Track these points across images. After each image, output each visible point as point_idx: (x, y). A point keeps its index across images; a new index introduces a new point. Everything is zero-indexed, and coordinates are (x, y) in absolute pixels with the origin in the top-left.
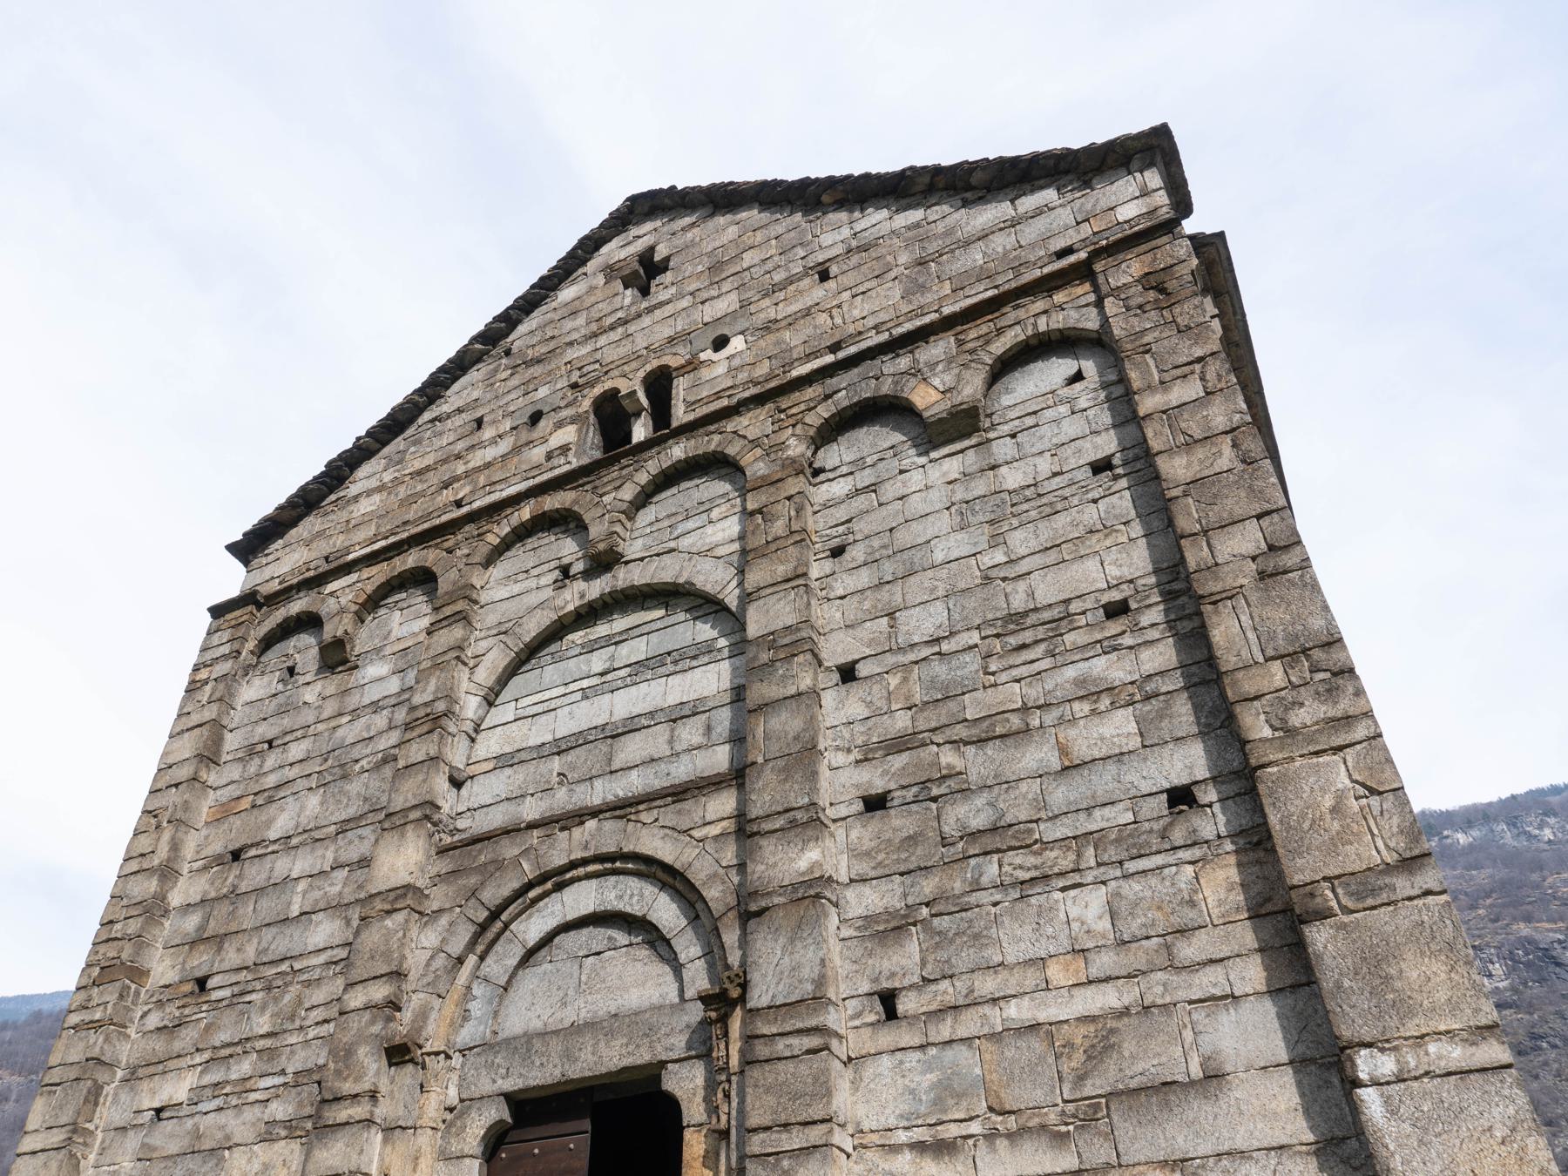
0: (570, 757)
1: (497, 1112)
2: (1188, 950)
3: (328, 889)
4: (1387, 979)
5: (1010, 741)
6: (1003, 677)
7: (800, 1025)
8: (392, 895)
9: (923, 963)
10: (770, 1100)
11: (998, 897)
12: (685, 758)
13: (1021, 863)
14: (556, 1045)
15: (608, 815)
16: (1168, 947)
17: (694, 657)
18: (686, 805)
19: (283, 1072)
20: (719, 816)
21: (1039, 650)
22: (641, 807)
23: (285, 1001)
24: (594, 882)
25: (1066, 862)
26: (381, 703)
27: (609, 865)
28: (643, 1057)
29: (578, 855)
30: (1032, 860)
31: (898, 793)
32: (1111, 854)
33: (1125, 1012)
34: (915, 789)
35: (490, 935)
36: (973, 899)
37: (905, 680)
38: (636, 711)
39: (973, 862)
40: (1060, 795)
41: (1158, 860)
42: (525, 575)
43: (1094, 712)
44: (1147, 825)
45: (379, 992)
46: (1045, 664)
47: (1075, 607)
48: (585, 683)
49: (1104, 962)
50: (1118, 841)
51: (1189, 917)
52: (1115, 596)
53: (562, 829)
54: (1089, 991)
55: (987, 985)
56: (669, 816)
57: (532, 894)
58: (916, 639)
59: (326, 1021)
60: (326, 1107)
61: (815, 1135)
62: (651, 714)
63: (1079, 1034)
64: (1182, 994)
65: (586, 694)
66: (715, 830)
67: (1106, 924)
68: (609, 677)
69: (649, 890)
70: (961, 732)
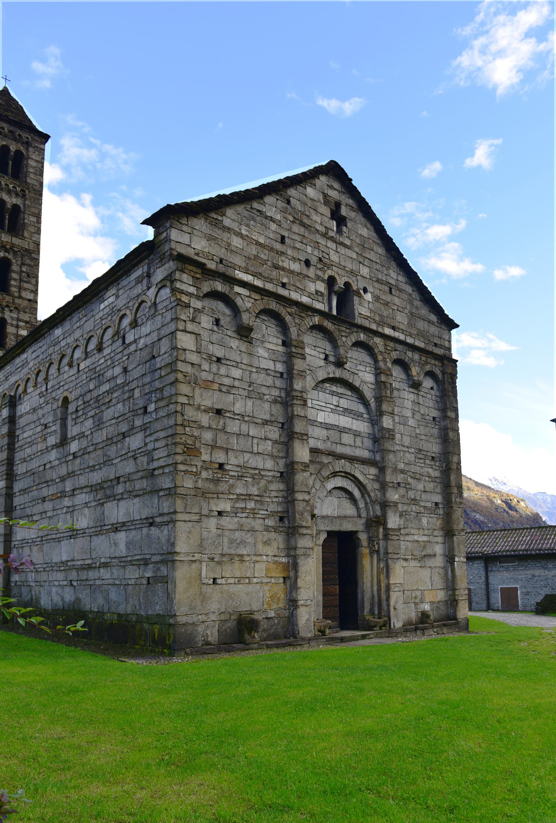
0: (331, 432)
6: (418, 464)
18: (365, 467)
19: (267, 510)
21: (422, 461)
22: (355, 462)
23: (261, 485)
24: (340, 478)
26: (268, 371)
29: (341, 470)
38: (346, 426)
42: (313, 348)
43: (428, 481)
45: (307, 497)
46: (423, 465)
47: (429, 454)
53: (337, 459)
58: (405, 445)
59: (277, 497)
62: (350, 429)
66: (372, 477)
70: (412, 475)
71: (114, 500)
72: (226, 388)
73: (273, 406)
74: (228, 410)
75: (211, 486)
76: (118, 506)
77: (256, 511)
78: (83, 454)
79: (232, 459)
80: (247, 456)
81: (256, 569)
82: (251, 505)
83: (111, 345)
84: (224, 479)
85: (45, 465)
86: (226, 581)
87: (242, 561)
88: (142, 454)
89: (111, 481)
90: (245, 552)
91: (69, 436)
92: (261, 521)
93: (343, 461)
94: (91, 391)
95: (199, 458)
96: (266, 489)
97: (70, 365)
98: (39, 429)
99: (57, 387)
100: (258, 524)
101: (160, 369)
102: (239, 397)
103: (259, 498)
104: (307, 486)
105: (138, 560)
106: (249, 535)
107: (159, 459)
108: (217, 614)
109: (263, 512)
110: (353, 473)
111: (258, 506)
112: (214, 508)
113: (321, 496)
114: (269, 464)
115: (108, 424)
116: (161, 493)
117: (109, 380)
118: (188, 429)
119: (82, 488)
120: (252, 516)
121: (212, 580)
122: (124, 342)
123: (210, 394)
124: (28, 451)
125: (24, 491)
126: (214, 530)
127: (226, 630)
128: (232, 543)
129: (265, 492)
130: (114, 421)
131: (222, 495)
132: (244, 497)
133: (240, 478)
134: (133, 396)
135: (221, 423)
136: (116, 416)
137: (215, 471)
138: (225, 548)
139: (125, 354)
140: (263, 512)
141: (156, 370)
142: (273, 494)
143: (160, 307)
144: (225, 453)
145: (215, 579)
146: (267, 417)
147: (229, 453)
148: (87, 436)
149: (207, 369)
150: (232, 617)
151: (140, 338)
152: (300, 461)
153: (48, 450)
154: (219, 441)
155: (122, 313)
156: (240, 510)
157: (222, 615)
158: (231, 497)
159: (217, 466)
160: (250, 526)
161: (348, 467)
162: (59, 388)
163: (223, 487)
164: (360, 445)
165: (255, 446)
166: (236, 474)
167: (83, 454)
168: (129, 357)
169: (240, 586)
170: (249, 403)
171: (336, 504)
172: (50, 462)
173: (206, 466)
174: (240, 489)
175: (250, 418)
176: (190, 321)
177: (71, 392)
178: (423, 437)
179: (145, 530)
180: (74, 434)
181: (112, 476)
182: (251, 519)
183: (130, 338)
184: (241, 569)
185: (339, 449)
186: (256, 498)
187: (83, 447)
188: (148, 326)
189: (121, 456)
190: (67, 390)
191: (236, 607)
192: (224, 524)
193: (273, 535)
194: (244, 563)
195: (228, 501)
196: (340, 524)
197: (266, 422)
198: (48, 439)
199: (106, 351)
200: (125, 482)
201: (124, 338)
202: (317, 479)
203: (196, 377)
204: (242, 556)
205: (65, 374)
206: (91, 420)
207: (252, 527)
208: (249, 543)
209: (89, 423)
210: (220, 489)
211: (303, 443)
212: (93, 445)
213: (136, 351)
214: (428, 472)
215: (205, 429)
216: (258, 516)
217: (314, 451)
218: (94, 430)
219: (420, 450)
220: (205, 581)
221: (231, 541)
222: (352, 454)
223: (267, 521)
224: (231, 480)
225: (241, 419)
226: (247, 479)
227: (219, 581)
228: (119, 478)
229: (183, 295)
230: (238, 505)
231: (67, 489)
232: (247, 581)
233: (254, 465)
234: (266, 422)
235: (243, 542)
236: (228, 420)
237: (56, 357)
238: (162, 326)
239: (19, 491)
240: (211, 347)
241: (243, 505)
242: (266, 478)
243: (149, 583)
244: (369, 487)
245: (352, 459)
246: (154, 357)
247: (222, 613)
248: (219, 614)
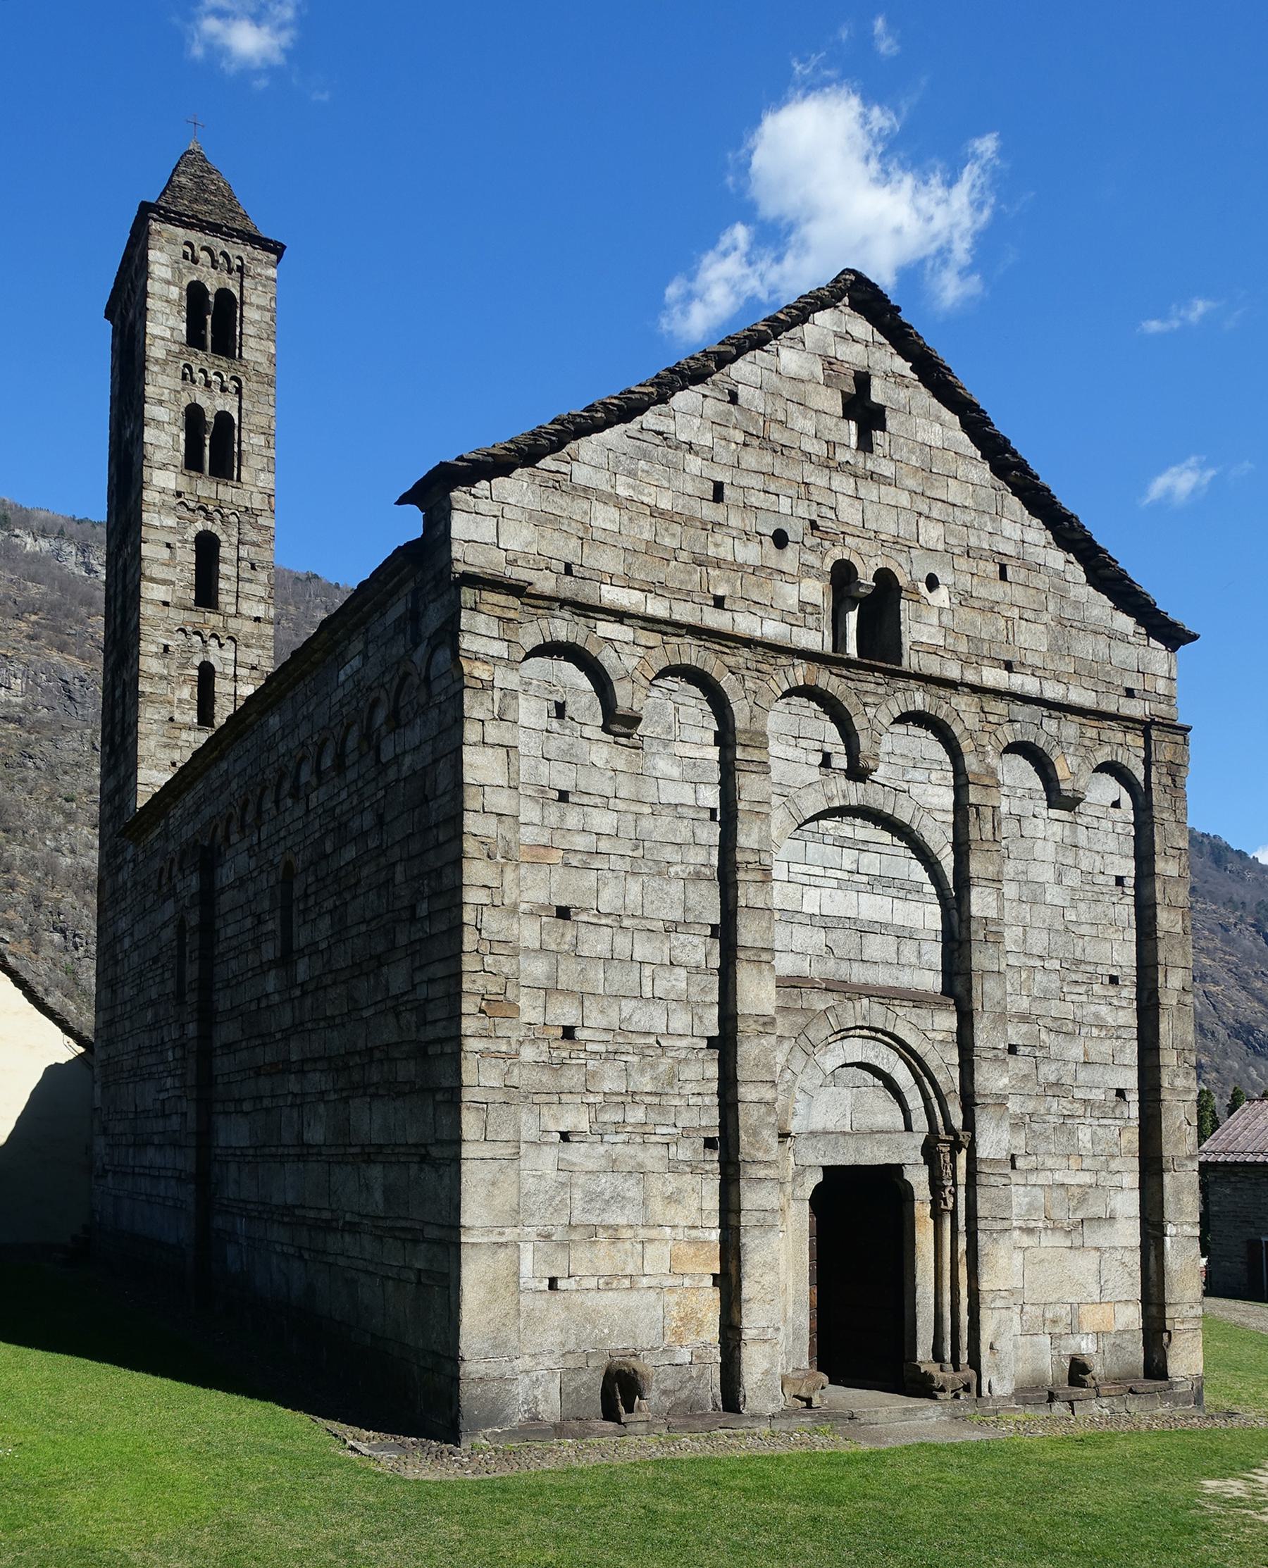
0: (837, 935)
1: (818, 1177)
2: (1114, 1165)
3: (674, 982)
4: (1179, 1200)
5: (1068, 1038)
7: (1001, 1172)
8: (762, 1020)
9: (1027, 1145)
10: (988, 1206)
11: (1056, 1120)
12: (907, 970)
13: (1064, 1106)
14: (851, 1142)
15: (876, 999)
16: (1107, 1161)
17: (909, 891)
20: (942, 1028)
21: (1082, 989)
22: (896, 1002)
23: (661, 1068)
25: (1081, 1112)
27: (873, 1034)
30: (1069, 1106)
31: (1022, 1048)
32: (1096, 1113)
33: (1091, 1186)
34: (1029, 1048)
36: (1047, 1118)
37: (1028, 977)
39: (1049, 1098)
40: (1083, 1075)
41: (1110, 1122)
44: (1108, 1104)
45: (768, 1094)
46: (1084, 998)
48: (839, 874)
49: (1088, 1163)
50: (1099, 1107)
51: (1115, 1150)
54: (1082, 1173)
55: (1050, 1162)
56: (913, 1014)
58: (1034, 952)
60: (748, 1166)
61: (1006, 1224)
63: (1077, 1191)
64: (1109, 1183)
65: (841, 885)
66: (940, 1037)
67: (1089, 1145)
68: (856, 877)
69: (894, 1056)
70: (1050, 1024)
71: (365, 1095)
72: (579, 857)
73: (691, 888)
74: (584, 906)
75: (546, 1078)
76: (370, 1109)
77: (648, 1129)
78: (317, 989)
79: (594, 1014)
80: (628, 1006)
81: (647, 1256)
82: (637, 1115)
83: (358, 762)
84: (574, 1061)
85: (259, 999)
86: (578, 1283)
87: (615, 1240)
88: (409, 1006)
89: (359, 1053)
90: (622, 1221)
91: (295, 947)
92: (662, 1151)
93: (865, 1001)
94: (329, 855)
95: (514, 1022)
96: (673, 1077)
97: (295, 793)
98: (248, 923)
99: (275, 839)
100: (652, 1157)
101: (437, 826)
102: (610, 875)
103: (656, 1100)
104: (769, 1068)
105: (403, 1229)
106: (632, 1181)
107: (436, 1021)
108: (558, 1353)
109: (665, 1130)
110: (890, 1030)
111: (654, 1117)
112: (551, 1127)
113: (808, 1085)
114: (680, 1021)
115: (354, 932)
116: (439, 1097)
117: (355, 839)
118: (489, 960)
119: (315, 1060)
120: (639, 1140)
121: (547, 1282)
122: (378, 760)
123: (542, 875)
124: (233, 965)
125: (230, 1047)
126: (550, 1172)
127: (576, 1390)
128: (592, 1200)
129: (670, 1084)
130: (363, 928)
131: (570, 1096)
132: (620, 1099)
133: (611, 1056)
134: (393, 879)
135: (568, 938)
136: (368, 915)
137: (554, 1045)
138: (576, 1212)
139: (381, 785)
140: (665, 1130)
141: (430, 828)
142: (689, 1088)
143: (436, 688)
144: (577, 1003)
145: (553, 1283)
146: (678, 915)
147: (587, 1003)
148: (322, 951)
149: (536, 821)
150: (592, 1363)
151: (404, 753)
152: (753, 1012)
153: (262, 969)
154: (563, 978)
155: (373, 695)
156: (612, 1128)
157: (569, 1356)
158: (591, 1099)
159: (560, 1032)
160: (633, 1163)
161: (878, 1015)
162: (278, 843)
163: (572, 1078)
164: (914, 960)
165: (647, 983)
166: (602, 1048)
167: (317, 989)
168: (386, 792)
169: (610, 1293)
170: (634, 887)
171: (848, 1102)
172: (267, 995)
173: (535, 1035)
174: (611, 1082)
175: (636, 921)
176: (494, 719)
177: (296, 854)
178: (1085, 930)
179: (414, 1169)
180: (302, 945)
181: (361, 1045)
182: (636, 1146)
183: (387, 753)
184: (611, 1258)
185: (860, 974)
186: (648, 1099)
187: (317, 973)
188: (417, 729)
189: (376, 1003)
190: (291, 848)
191: (602, 1341)
192: (574, 1160)
193: (688, 1180)
194: (619, 1245)
195: (584, 1108)
196: (857, 1150)
197: (672, 927)
198: (263, 946)
199: (351, 775)
200: (381, 1061)
201: (378, 750)
202: (797, 1049)
203: (508, 843)
204: (615, 1228)
205: (287, 813)
206: (327, 920)
207: (639, 1164)
208: (631, 1200)
209: (325, 924)
210: (565, 1083)
211: (760, 972)
212: (331, 972)
213: (397, 781)
214: (1096, 1015)
215: (532, 954)
216: (653, 1139)
217: (790, 984)
218: (332, 941)
219: (1077, 962)
220: (533, 1284)
221: (591, 1197)
222: (892, 983)
223: (673, 1148)
224: (591, 1063)
225: (616, 924)
226: (629, 1058)
227: (561, 1284)
228: (371, 1049)
229: (478, 664)
230: (606, 1117)
231: (294, 1058)
232: (627, 1283)
233: (644, 1025)
234: (672, 927)
235: (618, 1199)
236: (583, 929)
237: (270, 774)
238: (440, 733)
239: (221, 1047)
240: (544, 767)
241: (619, 1118)
242: (673, 1054)
243: (419, 1282)
244: (932, 1061)
245: (889, 996)
246: (426, 800)
247: (569, 1352)
248: (563, 1355)
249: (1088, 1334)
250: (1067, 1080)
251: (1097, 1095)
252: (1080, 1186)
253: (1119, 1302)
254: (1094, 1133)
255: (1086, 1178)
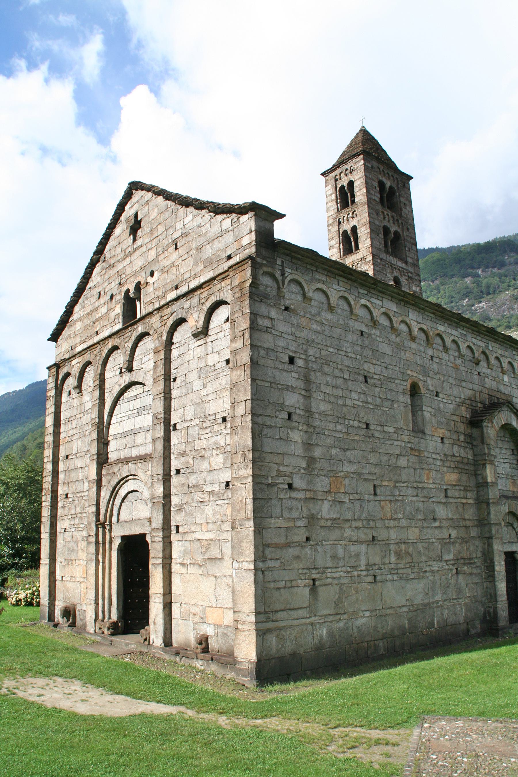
6: (202, 437)
21: (208, 431)
28: (142, 532)
30: (202, 496)
34: (185, 469)
35: (114, 494)
40: (209, 478)
51: (224, 518)
52: (224, 415)
57: (121, 483)
214: (216, 443)
219: (205, 417)
249: (210, 624)
250: (201, 482)
251: (216, 488)
252: (206, 540)
253: (226, 608)
254: (214, 510)
255: (210, 536)
